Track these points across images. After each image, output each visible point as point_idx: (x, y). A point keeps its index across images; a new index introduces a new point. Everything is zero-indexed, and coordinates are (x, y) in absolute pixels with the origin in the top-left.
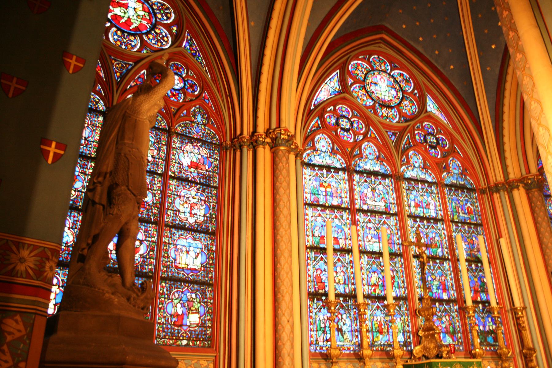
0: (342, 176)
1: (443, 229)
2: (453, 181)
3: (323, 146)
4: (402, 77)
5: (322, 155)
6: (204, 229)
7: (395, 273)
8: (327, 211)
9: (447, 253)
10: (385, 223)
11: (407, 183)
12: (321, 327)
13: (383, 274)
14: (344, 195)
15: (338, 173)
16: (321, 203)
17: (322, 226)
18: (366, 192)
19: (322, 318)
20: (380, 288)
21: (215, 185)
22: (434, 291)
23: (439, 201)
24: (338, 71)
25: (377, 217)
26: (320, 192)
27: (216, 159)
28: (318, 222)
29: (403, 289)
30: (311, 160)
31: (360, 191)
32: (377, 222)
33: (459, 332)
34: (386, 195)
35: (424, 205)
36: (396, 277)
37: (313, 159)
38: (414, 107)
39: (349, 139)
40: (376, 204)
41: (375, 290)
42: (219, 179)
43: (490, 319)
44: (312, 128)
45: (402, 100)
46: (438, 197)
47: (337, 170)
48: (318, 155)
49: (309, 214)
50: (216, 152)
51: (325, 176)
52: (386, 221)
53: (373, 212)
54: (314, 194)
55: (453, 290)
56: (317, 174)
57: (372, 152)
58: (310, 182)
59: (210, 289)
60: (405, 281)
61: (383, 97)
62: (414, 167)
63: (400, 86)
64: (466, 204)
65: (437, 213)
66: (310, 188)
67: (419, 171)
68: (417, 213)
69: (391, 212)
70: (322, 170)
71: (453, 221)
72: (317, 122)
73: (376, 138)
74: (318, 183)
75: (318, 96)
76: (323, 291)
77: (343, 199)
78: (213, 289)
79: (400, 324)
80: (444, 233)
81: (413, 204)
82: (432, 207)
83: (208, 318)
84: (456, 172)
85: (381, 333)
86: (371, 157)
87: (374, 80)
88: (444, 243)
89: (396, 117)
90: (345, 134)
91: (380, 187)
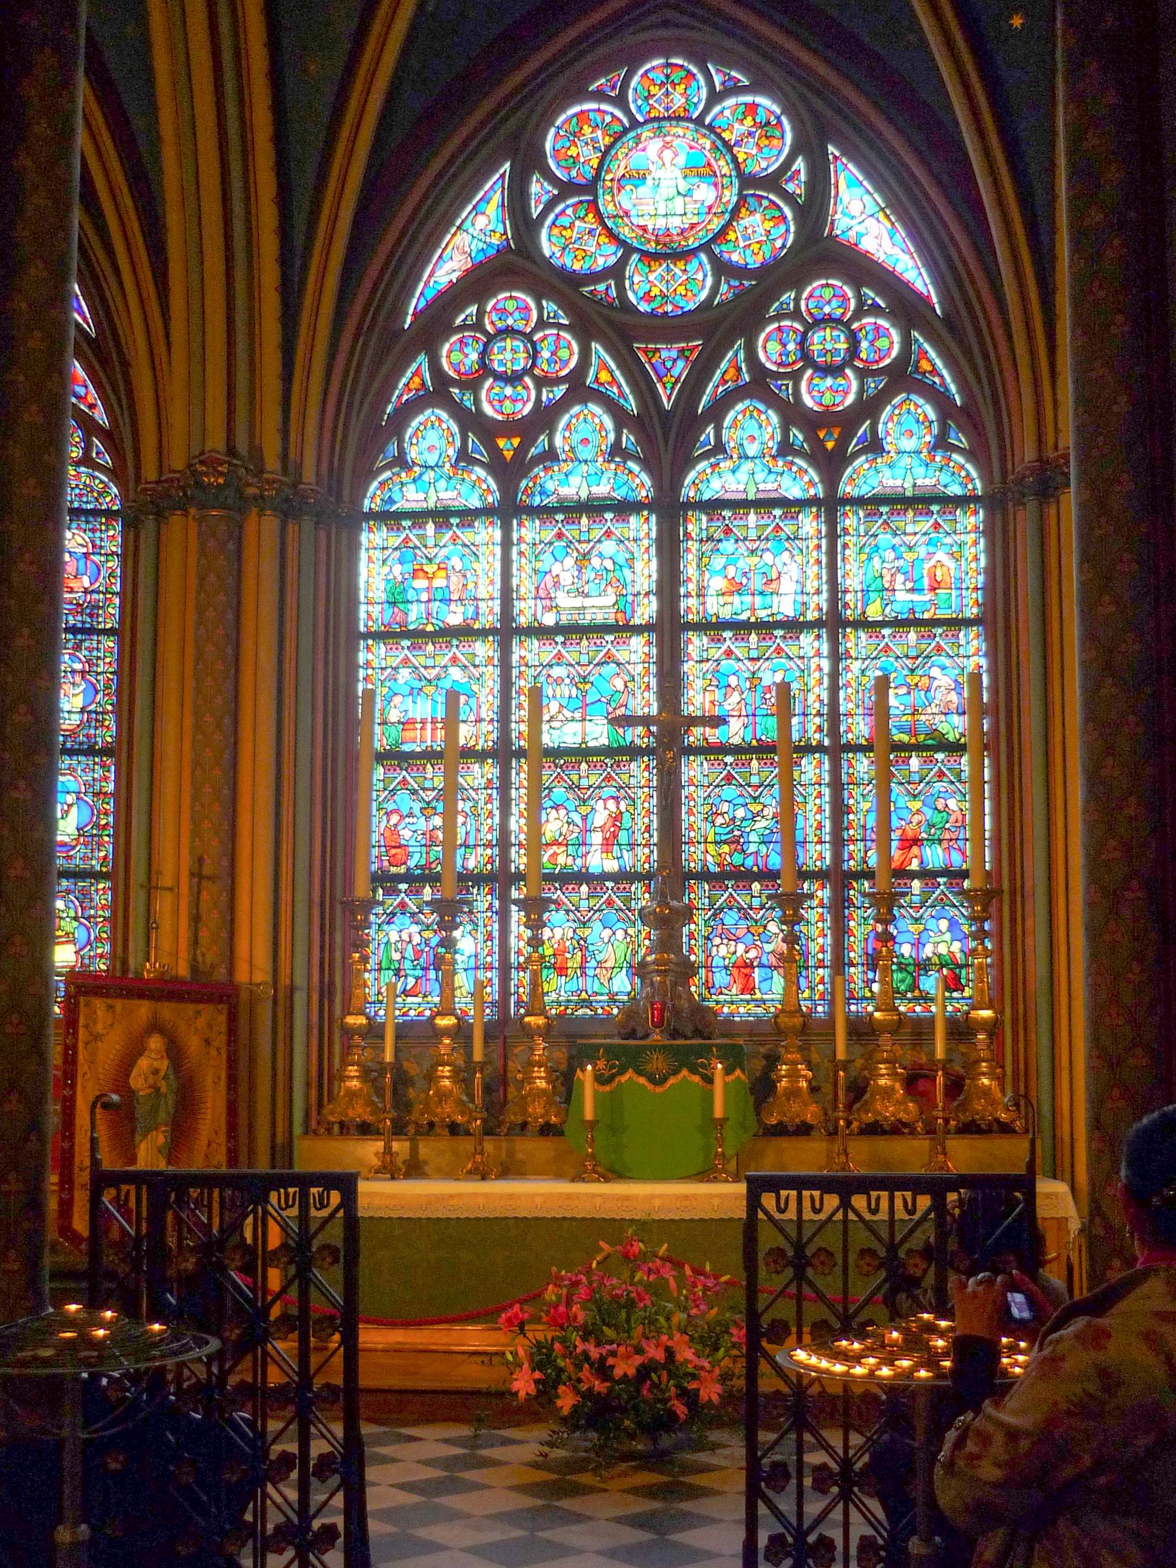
0: (487, 533)
1: (818, 654)
2: (891, 483)
3: (431, 449)
4: (749, 121)
5: (425, 478)
6: (81, 744)
7: (623, 807)
8: (430, 647)
9: (819, 729)
10: (609, 659)
11: (704, 518)
12: (391, 961)
13: (584, 810)
14: (482, 593)
15: (471, 525)
16: (411, 627)
17: (411, 694)
18: (557, 569)
19: (394, 936)
20: (571, 850)
21: (109, 626)
22: (752, 848)
23: (818, 562)
24: (507, 166)
25: (585, 642)
26: (411, 595)
27: (113, 553)
28: (401, 681)
29: (647, 851)
30: (391, 501)
31: (536, 571)
32: (584, 659)
33: (821, 965)
34: (626, 571)
35: (758, 583)
36: (626, 816)
37: (396, 496)
38: (782, 228)
39: (519, 406)
40: (588, 602)
41: (555, 854)
42: (122, 607)
43: (944, 924)
44: (400, 397)
45: (735, 213)
46: (819, 547)
47: (468, 516)
48: (414, 480)
49: (375, 664)
50: (111, 533)
51: (431, 542)
52: (614, 651)
53: (573, 631)
54: (393, 604)
55: (820, 842)
56: (407, 540)
57: (594, 438)
58: (386, 569)
59: (101, 886)
60: (655, 825)
61: (661, 223)
62: (744, 457)
63: (735, 159)
64: (930, 555)
65: (804, 604)
66: (382, 586)
67: (758, 469)
68: (726, 614)
69: (637, 621)
70: (422, 526)
71: (863, 624)
72: (417, 373)
73: (614, 381)
74: (409, 568)
75: (428, 281)
76: (403, 870)
77: (482, 604)
78: (108, 884)
79: (623, 947)
80: (819, 668)
81: (717, 583)
82: (788, 586)
83: (99, 951)
84: (908, 444)
85: (561, 971)
86: (585, 453)
87: (637, 160)
88: (811, 698)
89: (703, 287)
90: (508, 391)
91: (609, 547)
